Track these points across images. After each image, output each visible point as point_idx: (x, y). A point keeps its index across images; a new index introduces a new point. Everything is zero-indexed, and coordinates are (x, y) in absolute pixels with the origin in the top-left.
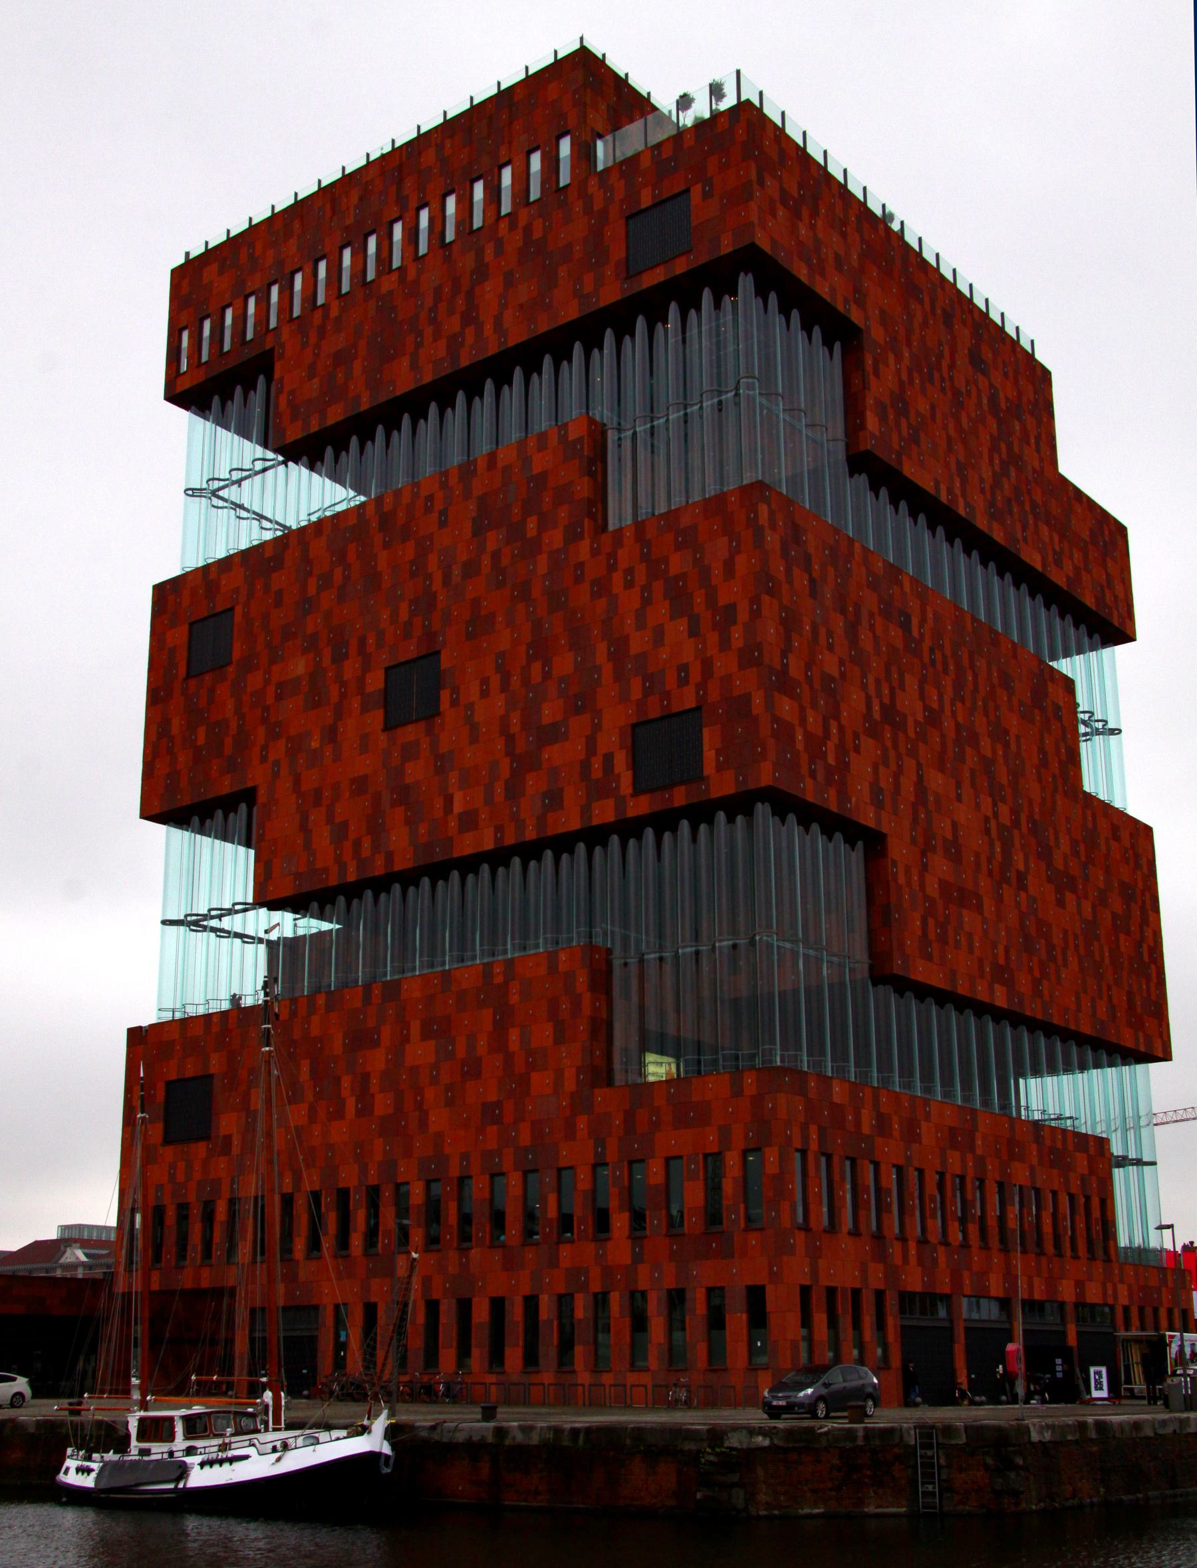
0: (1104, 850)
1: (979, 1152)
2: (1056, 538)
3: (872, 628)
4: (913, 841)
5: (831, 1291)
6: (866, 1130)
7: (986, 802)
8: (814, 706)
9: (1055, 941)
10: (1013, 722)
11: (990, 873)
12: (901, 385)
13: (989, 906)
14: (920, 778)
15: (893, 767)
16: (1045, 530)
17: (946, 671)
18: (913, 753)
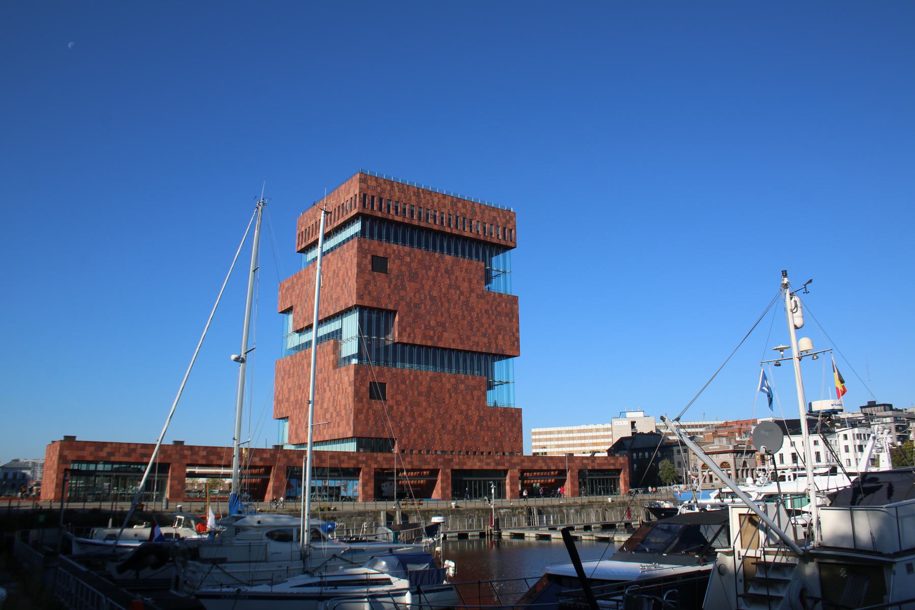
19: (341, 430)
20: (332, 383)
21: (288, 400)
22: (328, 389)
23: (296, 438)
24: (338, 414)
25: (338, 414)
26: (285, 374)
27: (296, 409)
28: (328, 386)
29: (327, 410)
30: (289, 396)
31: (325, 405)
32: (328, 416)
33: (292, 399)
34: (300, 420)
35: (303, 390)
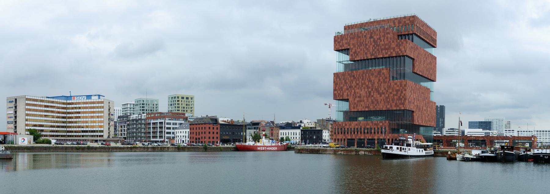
0: (392, 87)
1: (361, 125)
2: (387, 51)
3: (348, 79)
4: (353, 98)
5: (338, 139)
6: (344, 125)
7: (366, 90)
8: (339, 90)
9: (379, 101)
10: (372, 79)
11: (366, 97)
12: (356, 50)
13: (365, 101)
14: (355, 91)
15: (350, 92)
16: (384, 51)
17: (360, 78)
18: (354, 89)
19: (433, 123)
20: (430, 105)
21: (414, 103)
22: (429, 107)
23: (418, 122)
24: (432, 118)
25: (432, 118)
26: (412, 90)
27: (417, 109)
28: (429, 106)
29: (429, 115)
30: (414, 101)
31: (428, 112)
32: (429, 117)
33: (416, 104)
34: (419, 115)
35: (420, 102)
